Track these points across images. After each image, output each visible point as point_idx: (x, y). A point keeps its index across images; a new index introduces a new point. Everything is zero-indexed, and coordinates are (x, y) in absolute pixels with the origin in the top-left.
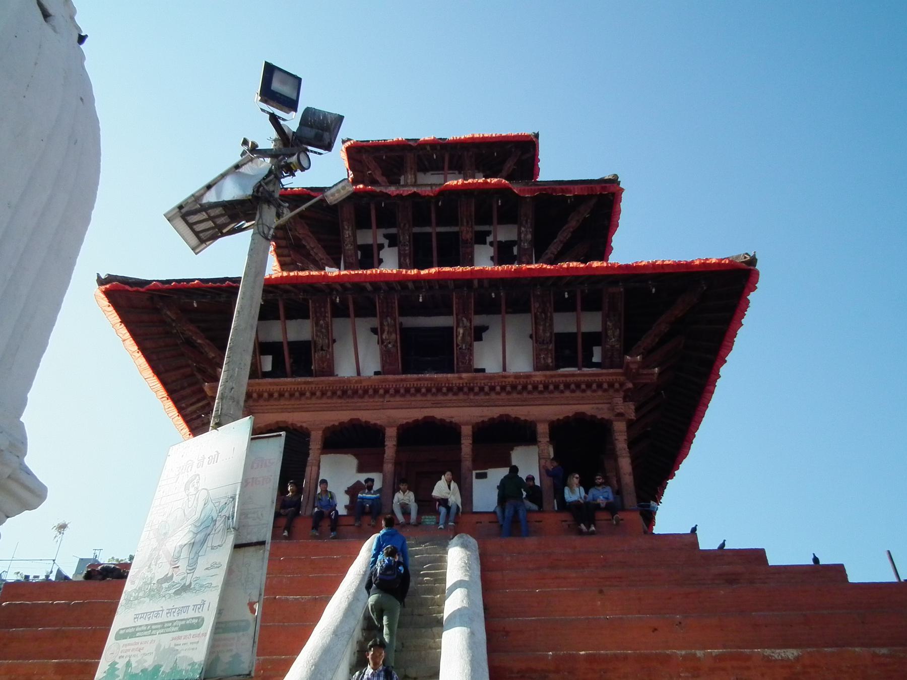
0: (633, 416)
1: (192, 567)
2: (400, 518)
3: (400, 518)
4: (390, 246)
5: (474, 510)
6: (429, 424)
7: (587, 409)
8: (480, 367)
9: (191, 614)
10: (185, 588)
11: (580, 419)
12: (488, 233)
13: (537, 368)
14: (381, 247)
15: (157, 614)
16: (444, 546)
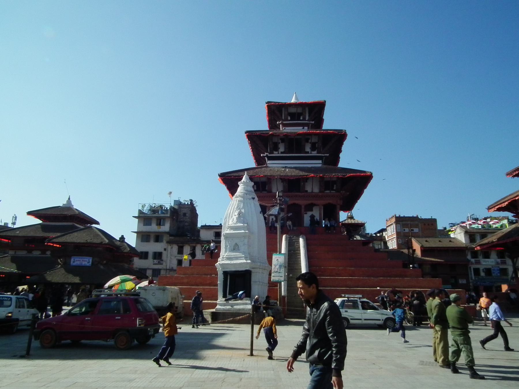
0: (342, 204)
1: (280, 270)
2: (289, 228)
3: (289, 228)
4: (282, 142)
5: (305, 226)
6: (294, 204)
7: (331, 201)
8: (307, 190)
9: (281, 275)
10: (279, 273)
11: (329, 204)
12: (309, 139)
13: (320, 192)
14: (279, 143)
15: (277, 275)
16: (298, 237)
